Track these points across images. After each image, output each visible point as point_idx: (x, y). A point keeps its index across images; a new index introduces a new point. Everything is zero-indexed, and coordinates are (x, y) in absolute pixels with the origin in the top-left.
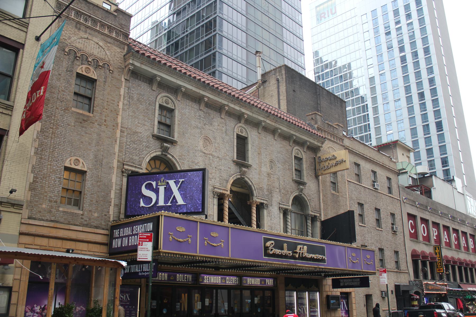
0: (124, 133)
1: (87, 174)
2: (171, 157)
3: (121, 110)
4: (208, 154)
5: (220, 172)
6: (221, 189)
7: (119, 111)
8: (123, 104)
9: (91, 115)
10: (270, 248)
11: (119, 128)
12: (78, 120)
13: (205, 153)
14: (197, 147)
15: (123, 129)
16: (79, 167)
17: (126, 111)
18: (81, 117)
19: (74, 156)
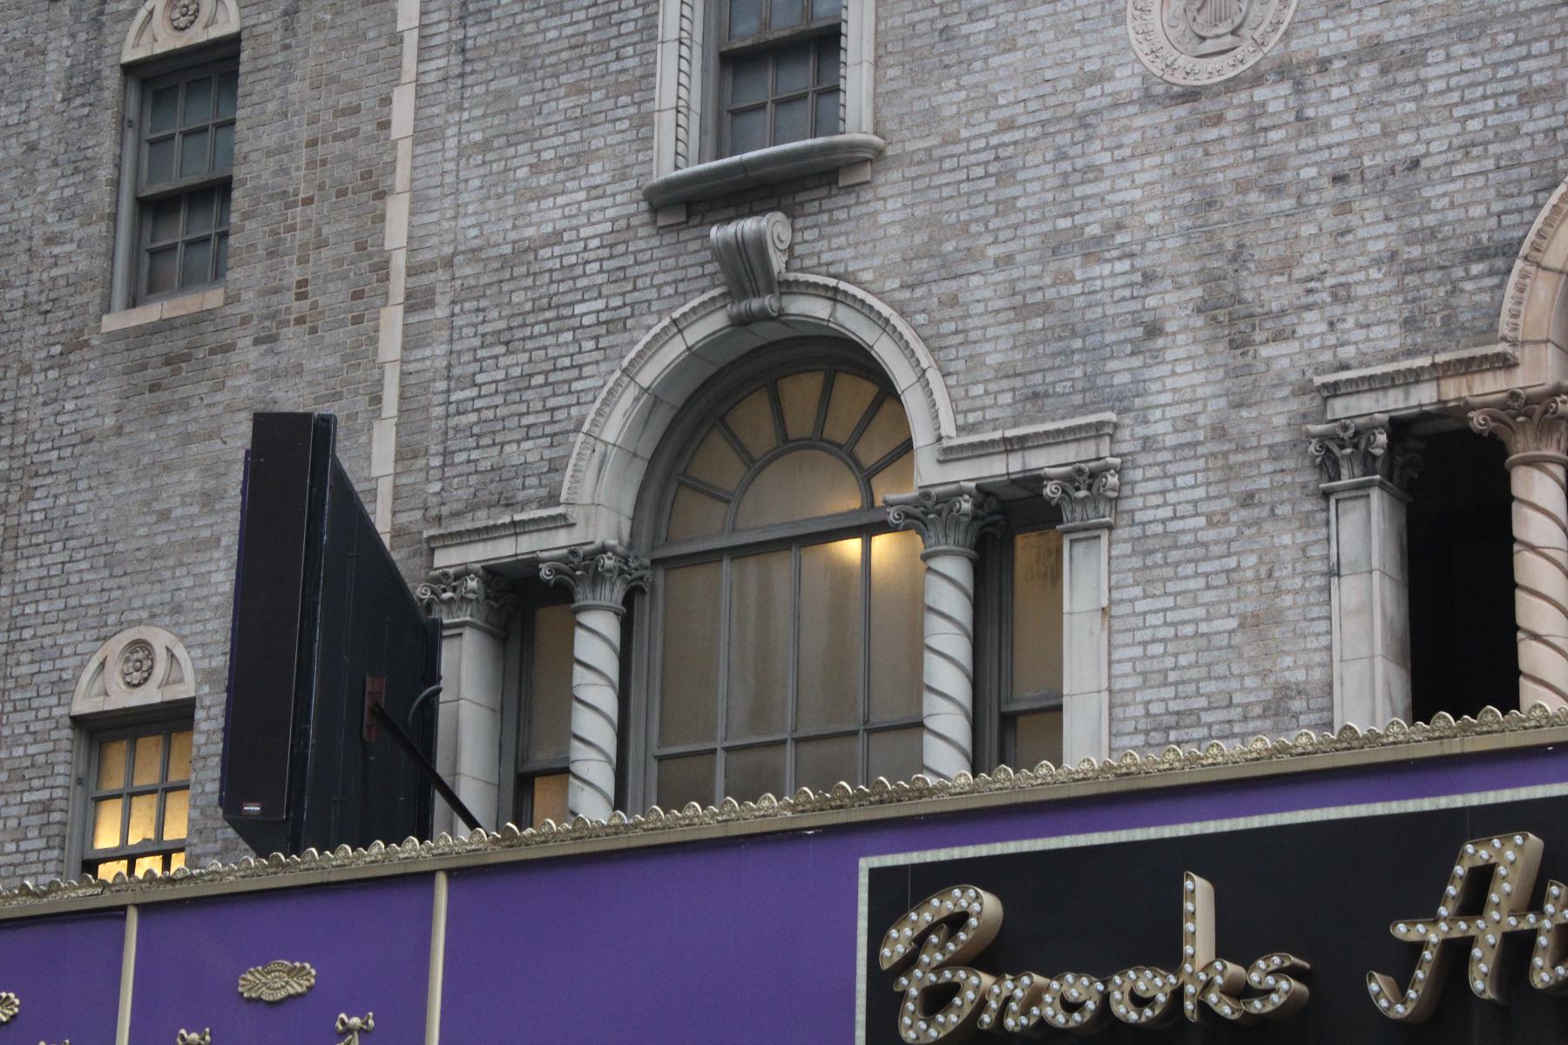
0: (431, 304)
1: (199, 714)
2: (818, 309)
3: (404, 149)
4: (1232, 85)
5: (1408, 202)
6: (1414, 377)
7: (391, 167)
8: (420, 86)
9: (213, 298)
10: (912, 986)
11: (398, 285)
12: (137, 378)
13: (1191, 95)
14: (1099, 78)
15: (426, 280)
16: (150, 695)
17: (442, 129)
18: (156, 349)
19: (122, 625)
